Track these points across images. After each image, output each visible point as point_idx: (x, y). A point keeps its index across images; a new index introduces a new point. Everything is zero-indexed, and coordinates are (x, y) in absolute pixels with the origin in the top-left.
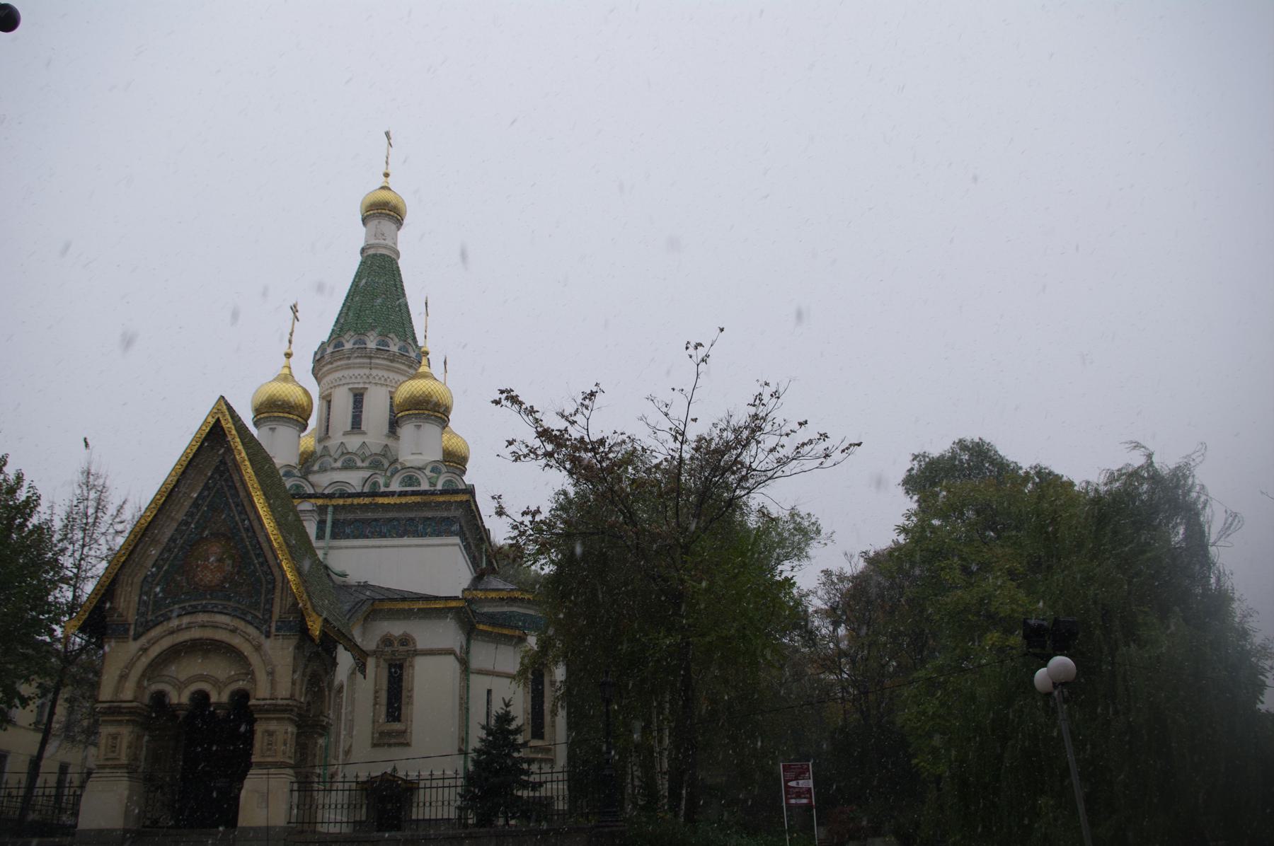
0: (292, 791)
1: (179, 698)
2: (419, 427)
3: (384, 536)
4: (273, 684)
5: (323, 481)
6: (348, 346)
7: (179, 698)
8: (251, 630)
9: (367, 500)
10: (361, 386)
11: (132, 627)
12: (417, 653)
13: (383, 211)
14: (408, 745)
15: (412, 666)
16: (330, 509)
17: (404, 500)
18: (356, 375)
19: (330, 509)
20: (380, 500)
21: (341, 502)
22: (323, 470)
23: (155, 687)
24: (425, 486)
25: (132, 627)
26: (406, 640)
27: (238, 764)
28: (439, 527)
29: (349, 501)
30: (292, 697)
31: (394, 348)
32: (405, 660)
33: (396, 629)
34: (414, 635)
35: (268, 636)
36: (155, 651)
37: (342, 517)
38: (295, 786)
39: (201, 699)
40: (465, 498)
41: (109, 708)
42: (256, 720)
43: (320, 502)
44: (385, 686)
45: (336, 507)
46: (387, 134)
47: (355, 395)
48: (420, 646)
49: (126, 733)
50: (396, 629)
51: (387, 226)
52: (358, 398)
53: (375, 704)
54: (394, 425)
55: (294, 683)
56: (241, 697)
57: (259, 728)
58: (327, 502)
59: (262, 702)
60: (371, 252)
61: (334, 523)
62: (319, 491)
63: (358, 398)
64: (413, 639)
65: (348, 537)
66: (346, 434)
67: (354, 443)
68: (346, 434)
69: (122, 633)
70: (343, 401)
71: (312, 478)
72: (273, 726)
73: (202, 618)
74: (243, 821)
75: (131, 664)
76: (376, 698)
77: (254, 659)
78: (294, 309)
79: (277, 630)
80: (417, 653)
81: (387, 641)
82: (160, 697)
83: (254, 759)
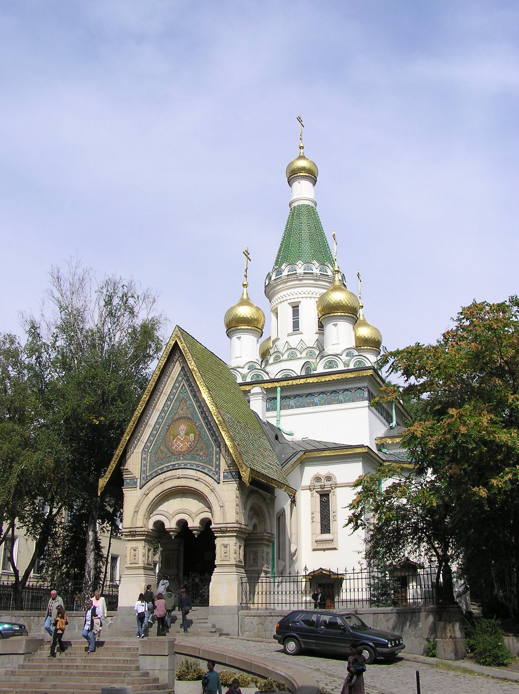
0: (242, 583)
1: (171, 525)
3: (316, 405)
4: (224, 514)
5: (274, 371)
6: (285, 273)
7: (171, 525)
8: (208, 478)
10: (296, 300)
11: (139, 480)
12: (336, 486)
14: (335, 549)
16: (279, 389)
19: (279, 389)
21: (285, 383)
22: (277, 360)
23: (155, 518)
24: (341, 367)
25: (139, 480)
26: (329, 478)
27: (208, 567)
29: (290, 382)
31: (316, 271)
33: (322, 470)
35: (219, 483)
36: (153, 495)
38: (245, 580)
39: (183, 524)
41: (130, 532)
42: (216, 538)
43: (270, 385)
44: (318, 509)
45: (283, 388)
46: (299, 119)
47: (293, 307)
48: (339, 480)
49: (141, 547)
52: (296, 308)
53: (313, 522)
54: (321, 326)
56: (206, 523)
57: (218, 542)
58: (277, 384)
59: (219, 526)
60: (295, 204)
62: (272, 377)
63: (296, 308)
66: (289, 335)
67: (294, 341)
69: (133, 485)
70: (286, 312)
71: (268, 369)
72: (226, 541)
73: (180, 472)
74: (213, 601)
75: (140, 503)
76: (313, 518)
77: (211, 498)
78: (246, 253)
79: (225, 477)
80: (336, 486)
81: (318, 479)
82: (159, 525)
83: (217, 562)
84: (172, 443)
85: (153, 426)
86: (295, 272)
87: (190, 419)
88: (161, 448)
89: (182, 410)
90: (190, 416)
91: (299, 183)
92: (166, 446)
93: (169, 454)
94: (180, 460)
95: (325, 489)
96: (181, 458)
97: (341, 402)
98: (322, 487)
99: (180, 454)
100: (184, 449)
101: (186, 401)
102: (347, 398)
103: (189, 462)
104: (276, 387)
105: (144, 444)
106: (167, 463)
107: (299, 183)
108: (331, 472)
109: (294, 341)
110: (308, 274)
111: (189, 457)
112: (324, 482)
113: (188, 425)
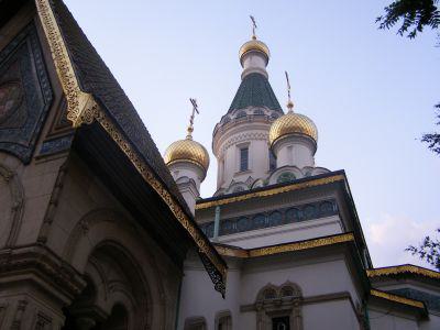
2: (290, 148)
9: (249, 196)
12: (303, 301)
13: (255, 51)
15: (300, 317)
16: (218, 208)
17: (282, 190)
18: (241, 136)
19: (218, 208)
20: (261, 194)
21: (226, 201)
26: (288, 289)
28: (319, 210)
30: (42, 241)
32: (291, 310)
33: (277, 278)
34: (299, 284)
37: (225, 217)
40: (338, 178)
50: (277, 278)
51: (259, 61)
55: (48, 221)
58: (215, 203)
61: (222, 223)
63: (244, 152)
64: (297, 287)
65: (236, 232)
67: (243, 178)
68: (237, 174)
70: (233, 154)
78: (193, 102)
80: (303, 301)
81: (269, 292)
87: (18, 80)
95: (284, 308)
97: (300, 220)
98: (279, 304)
102: (309, 215)
104: (215, 207)
108: (293, 280)
109: (243, 178)
110: (259, 114)
112: (279, 296)
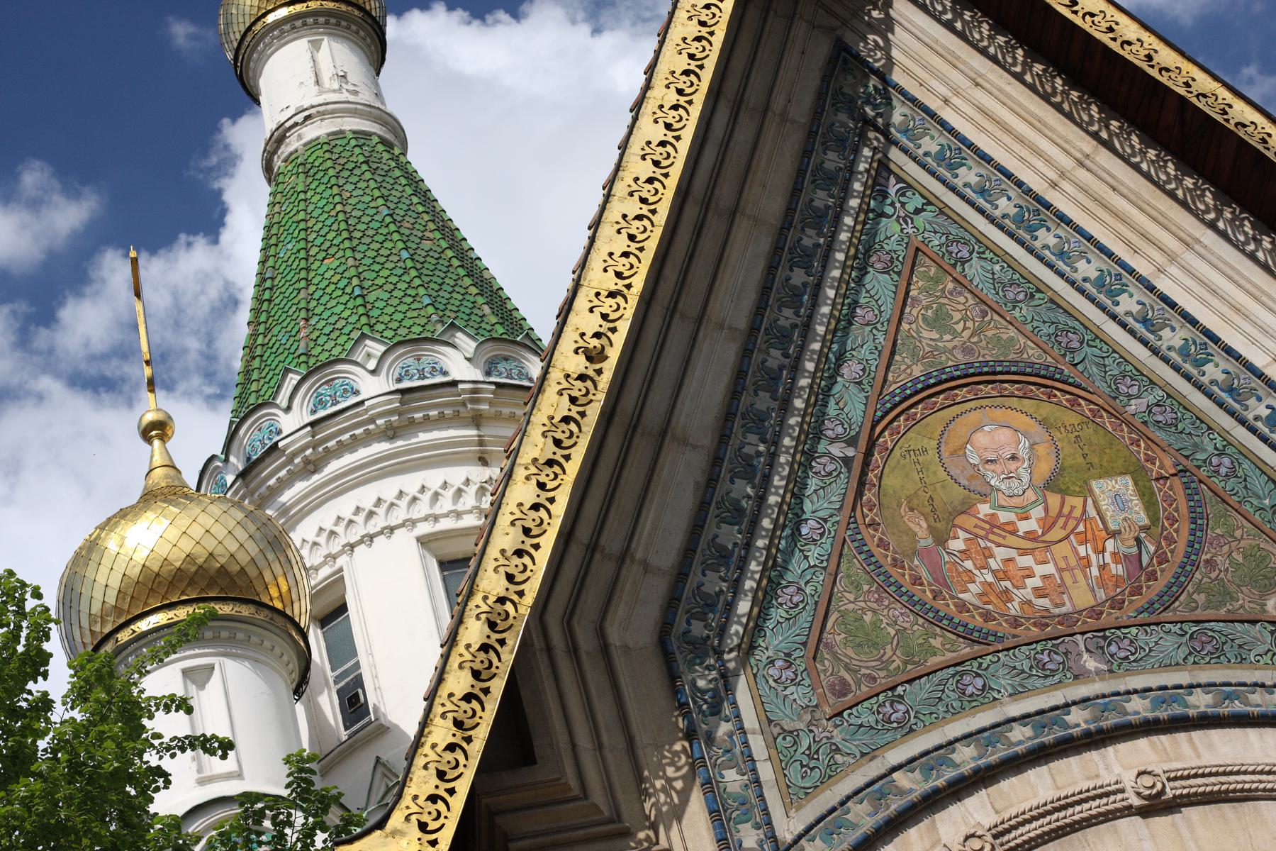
47: (444, 565)
84: (936, 569)
85: (706, 440)
86: (439, 379)
88: (847, 601)
89: (939, 321)
90: (1033, 354)
91: (316, 45)
92: (887, 586)
93: (944, 648)
94: (1080, 676)
96: (1091, 664)
99: (1053, 639)
100: (1081, 596)
101: (952, 266)
103: (1183, 678)
105: (656, 589)
106: (955, 713)
107: (316, 45)
111: (1167, 643)
113: (1044, 423)
